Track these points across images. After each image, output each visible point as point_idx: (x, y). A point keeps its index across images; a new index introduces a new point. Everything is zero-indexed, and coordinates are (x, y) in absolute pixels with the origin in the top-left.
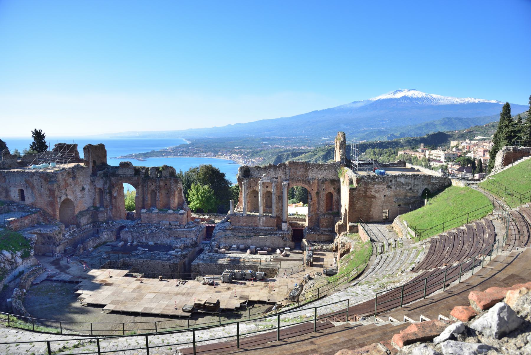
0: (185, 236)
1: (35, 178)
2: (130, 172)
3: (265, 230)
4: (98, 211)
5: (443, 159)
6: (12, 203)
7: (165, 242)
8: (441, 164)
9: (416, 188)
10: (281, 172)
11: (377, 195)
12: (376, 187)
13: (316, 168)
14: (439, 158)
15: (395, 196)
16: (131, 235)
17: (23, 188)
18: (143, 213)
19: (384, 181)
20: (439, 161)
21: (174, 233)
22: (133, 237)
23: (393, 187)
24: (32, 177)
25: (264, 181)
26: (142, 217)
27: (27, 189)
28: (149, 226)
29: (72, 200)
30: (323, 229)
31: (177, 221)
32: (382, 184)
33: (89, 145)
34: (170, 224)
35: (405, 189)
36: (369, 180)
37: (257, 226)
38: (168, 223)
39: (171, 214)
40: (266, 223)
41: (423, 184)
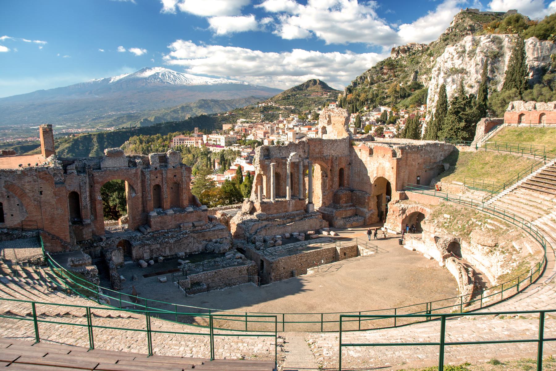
0: (216, 236)
1: (27, 179)
3: (298, 215)
4: (83, 225)
5: (223, 144)
7: (195, 249)
8: (223, 149)
10: (301, 150)
13: (331, 144)
14: (218, 143)
15: (424, 163)
16: (150, 249)
18: (154, 217)
20: (219, 146)
21: (204, 236)
22: (152, 251)
23: (423, 155)
25: (293, 161)
26: (152, 223)
28: (167, 233)
30: (345, 205)
31: (199, 221)
34: (194, 225)
37: (286, 212)
38: (192, 225)
39: (192, 212)
40: (295, 206)
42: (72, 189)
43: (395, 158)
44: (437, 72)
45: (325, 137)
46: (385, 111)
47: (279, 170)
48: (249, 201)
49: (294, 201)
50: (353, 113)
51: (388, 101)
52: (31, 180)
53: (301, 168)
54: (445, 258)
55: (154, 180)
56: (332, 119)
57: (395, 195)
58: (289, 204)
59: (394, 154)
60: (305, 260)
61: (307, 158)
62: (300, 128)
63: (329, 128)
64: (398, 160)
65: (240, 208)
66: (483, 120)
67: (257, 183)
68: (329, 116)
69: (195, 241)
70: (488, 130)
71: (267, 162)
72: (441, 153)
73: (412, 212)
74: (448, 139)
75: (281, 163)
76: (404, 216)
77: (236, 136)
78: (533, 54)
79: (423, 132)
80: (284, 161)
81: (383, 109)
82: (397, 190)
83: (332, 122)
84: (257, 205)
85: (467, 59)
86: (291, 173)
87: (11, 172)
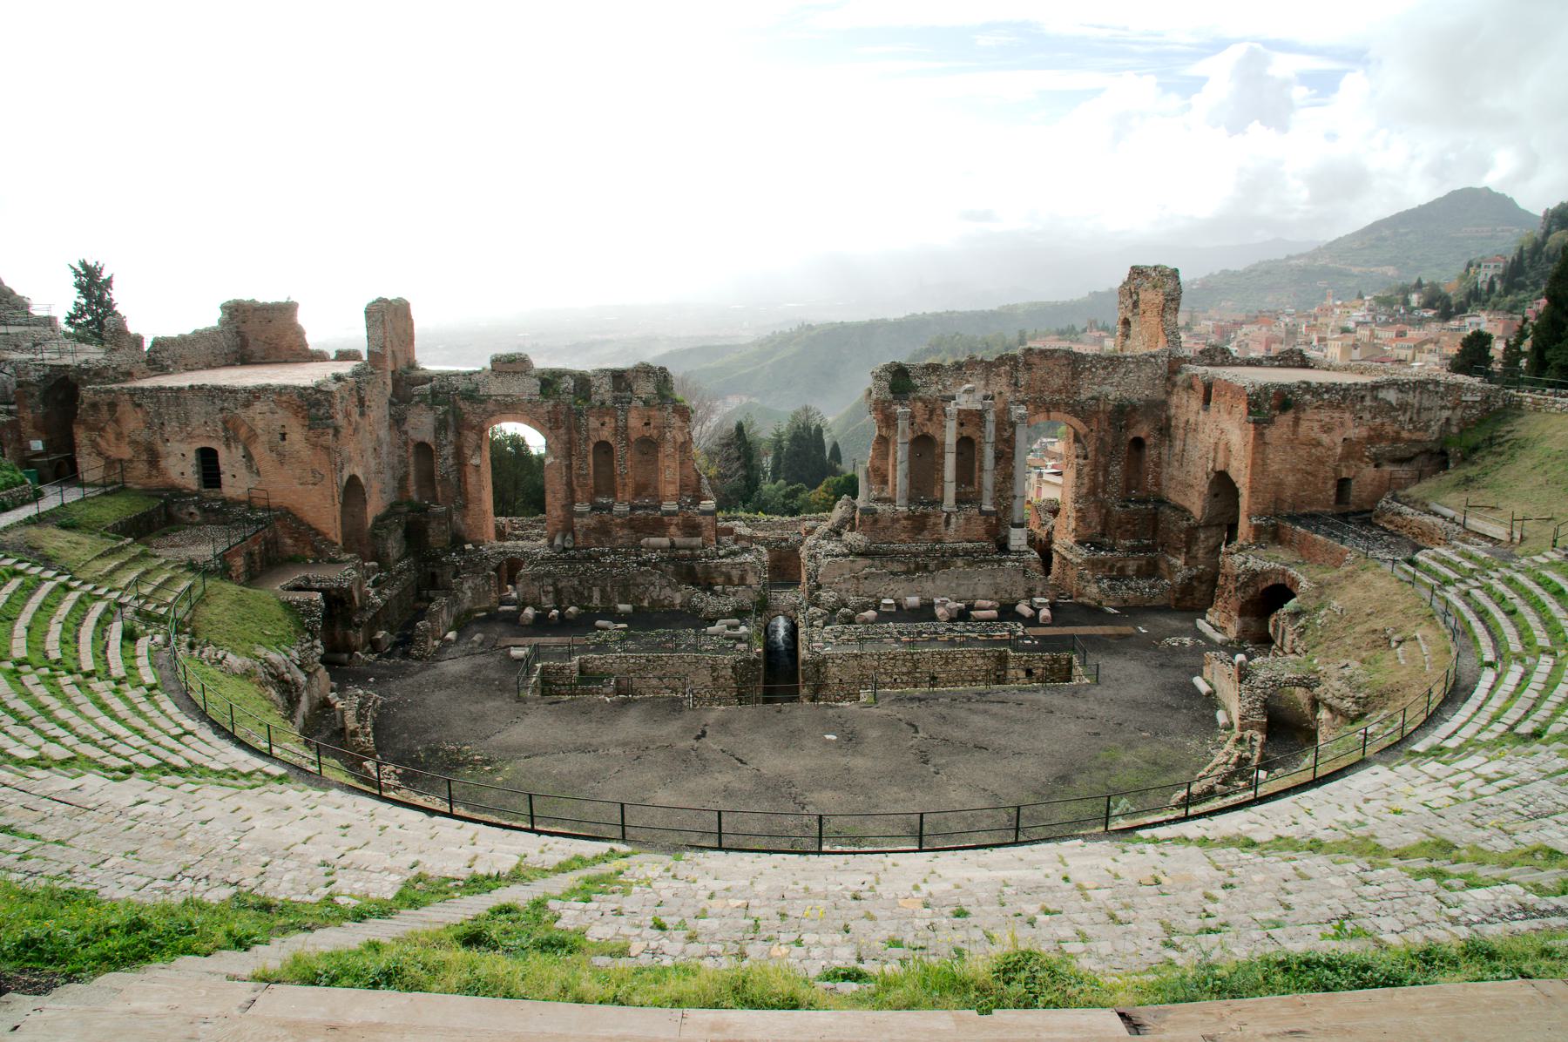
1: (258, 406)
2: (526, 388)
6: (174, 494)
9: (1425, 416)
10: (1004, 380)
11: (1325, 439)
12: (1324, 415)
13: (1104, 368)
15: (1371, 440)
16: (554, 584)
17: (213, 445)
18: (582, 515)
19: (1344, 398)
23: (1367, 416)
24: (247, 405)
27: (228, 446)
28: (603, 554)
29: (363, 480)
32: (1338, 407)
33: (381, 300)
35: (1395, 420)
36: (1308, 397)
41: (1442, 408)
42: (419, 437)
47: (930, 429)
52: (265, 408)
55: (596, 430)
58: (947, 523)
61: (1023, 402)
62: (1372, 331)
69: (664, 583)
72: (1446, 413)
75: (934, 409)
76: (1251, 591)
87: (234, 391)
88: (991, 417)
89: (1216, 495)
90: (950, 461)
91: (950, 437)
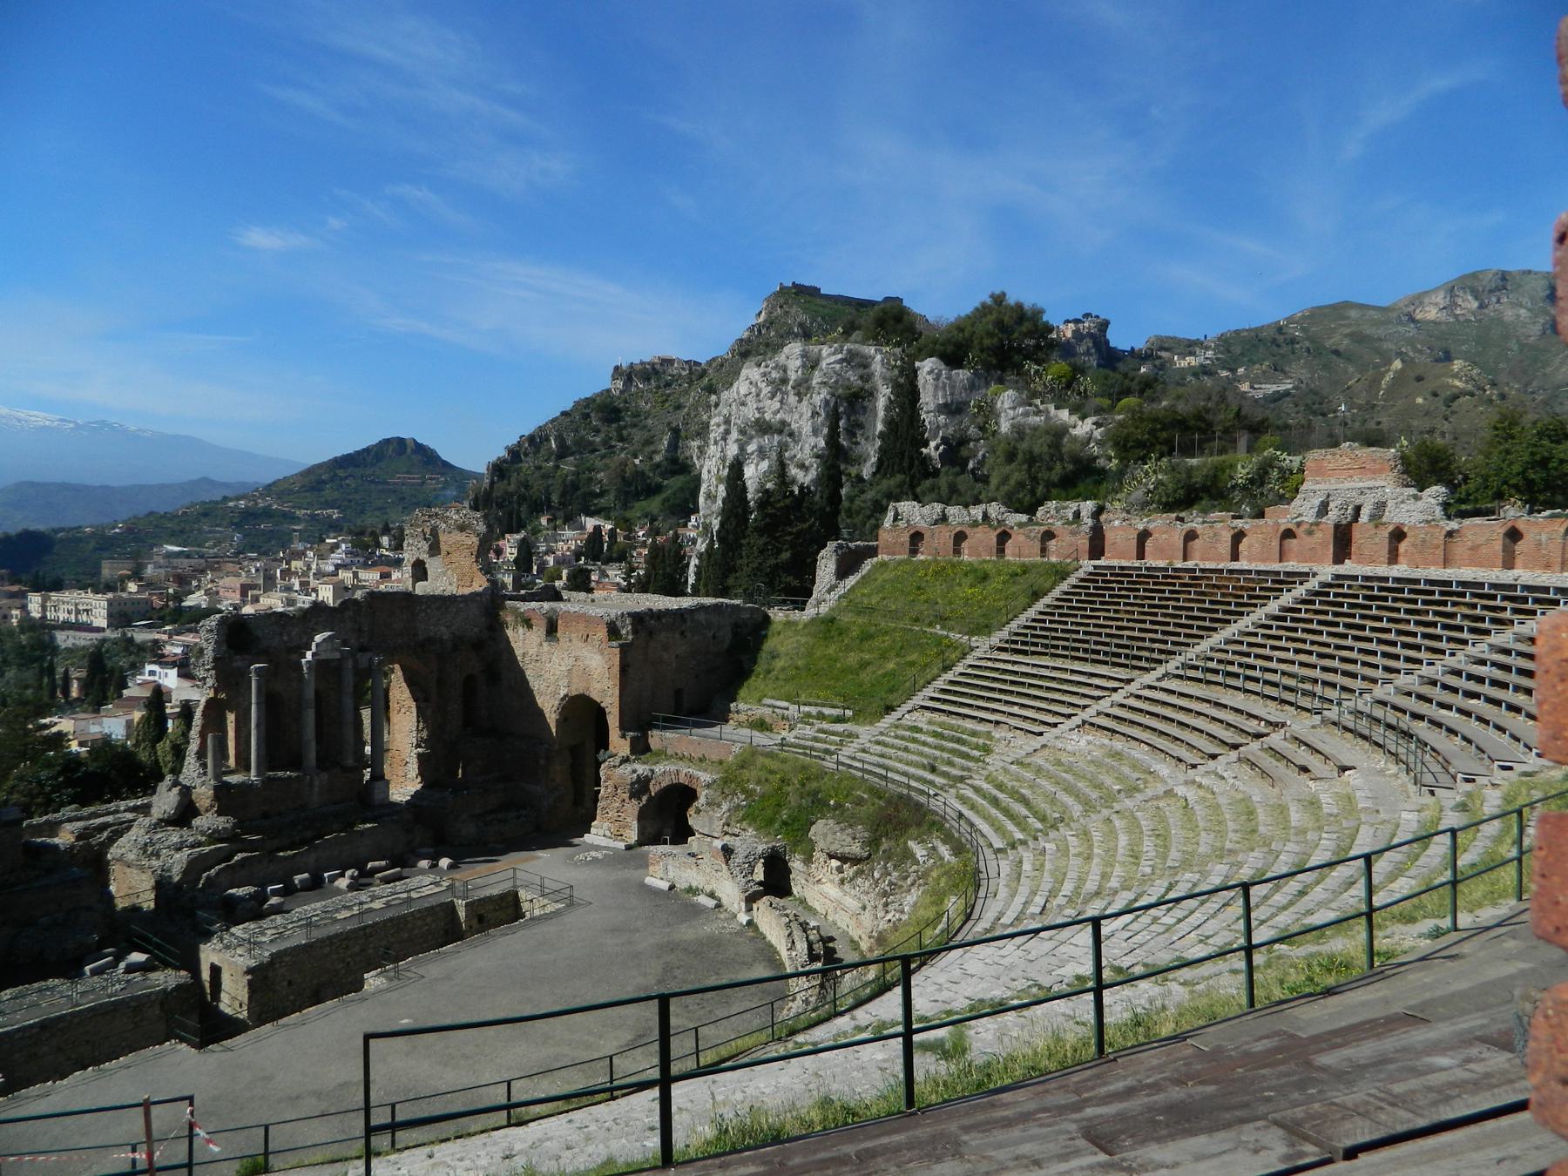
8: (99, 636)
11: (666, 656)
13: (438, 609)
14: (84, 618)
25: (323, 656)
43: (615, 644)
44: (722, 428)
45: (421, 588)
46: (597, 529)
48: (176, 783)
49: (325, 776)
50: (511, 532)
51: (603, 502)
53: (349, 678)
54: (751, 900)
56: (442, 538)
57: (619, 744)
59: (613, 631)
60: (357, 949)
62: (355, 575)
63: (433, 566)
64: (624, 649)
65: (145, 810)
66: (831, 545)
67: (203, 727)
68: (434, 532)
70: (843, 572)
71: (238, 663)
73: (664, 785)
74: (749, 596)
75: (283, 662)
77: (145, 596)
78: (935, 396)
79: (691, 580)
80: (294, 657)
81: (590, 523)
82: (624, 727)
83: (444, 547)
84: (203, 794)
85: (792, 399)
86: (317, 693)
88: (350, 664)
89: (565, 719)
90: (310, 716)
91: (310, 693)
